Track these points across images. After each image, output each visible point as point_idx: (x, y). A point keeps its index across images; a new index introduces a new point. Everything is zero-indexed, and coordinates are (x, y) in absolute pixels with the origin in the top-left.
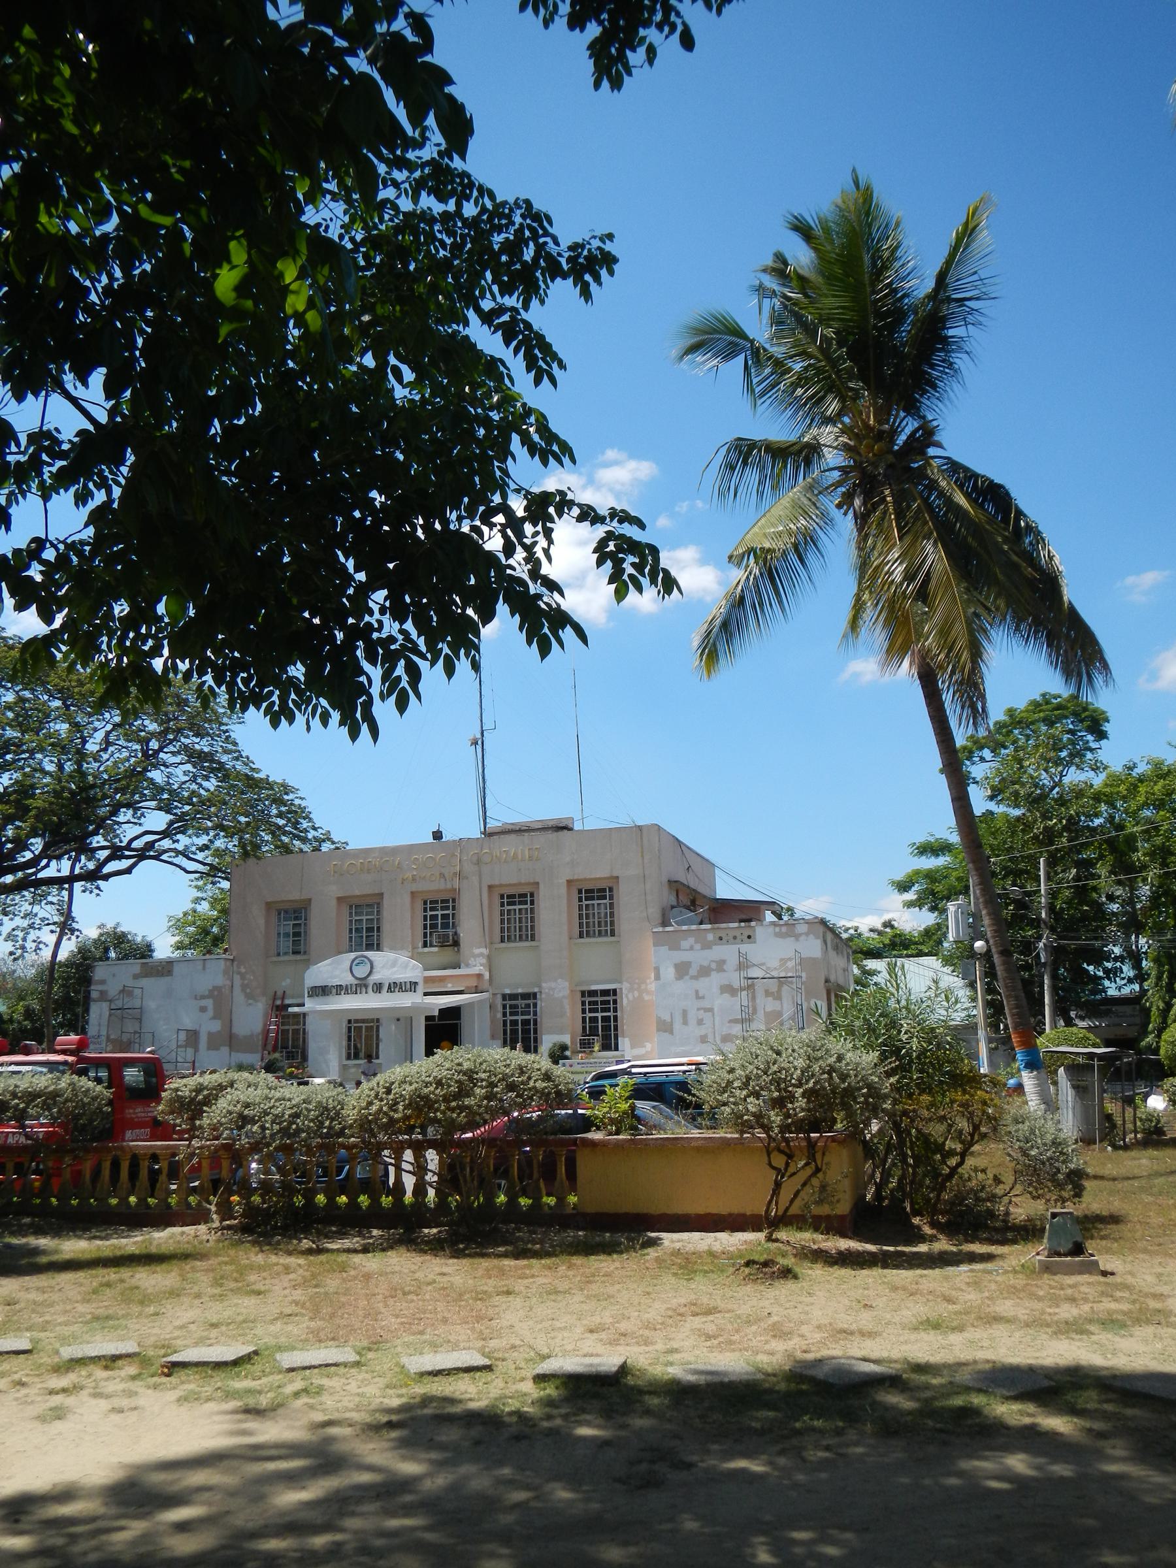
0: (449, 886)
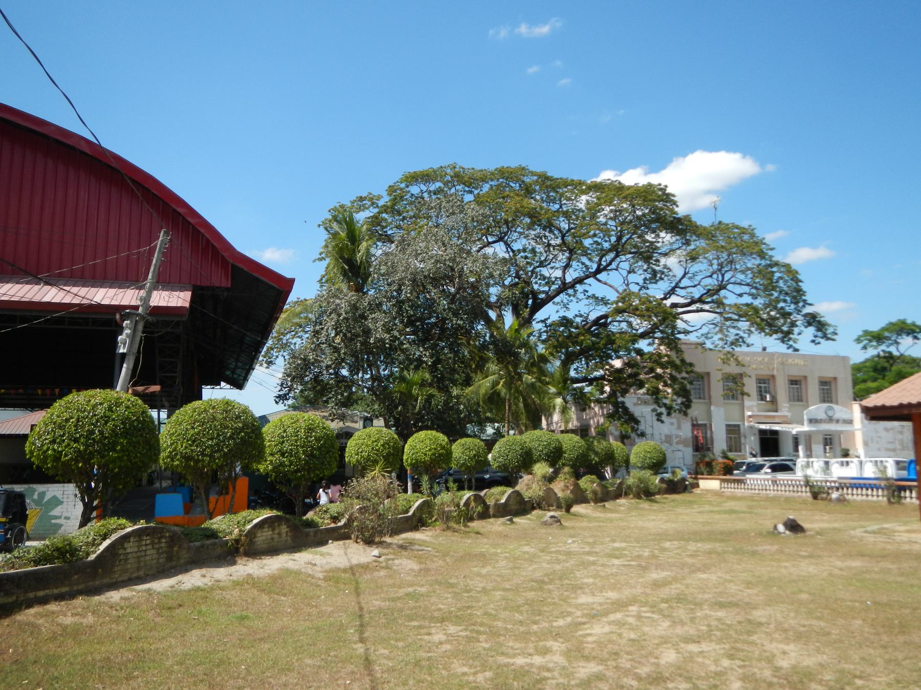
0: (771, 373)
